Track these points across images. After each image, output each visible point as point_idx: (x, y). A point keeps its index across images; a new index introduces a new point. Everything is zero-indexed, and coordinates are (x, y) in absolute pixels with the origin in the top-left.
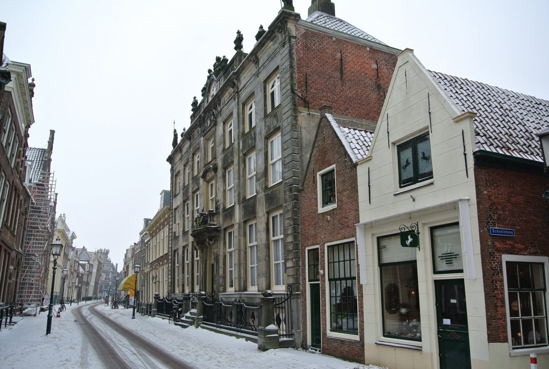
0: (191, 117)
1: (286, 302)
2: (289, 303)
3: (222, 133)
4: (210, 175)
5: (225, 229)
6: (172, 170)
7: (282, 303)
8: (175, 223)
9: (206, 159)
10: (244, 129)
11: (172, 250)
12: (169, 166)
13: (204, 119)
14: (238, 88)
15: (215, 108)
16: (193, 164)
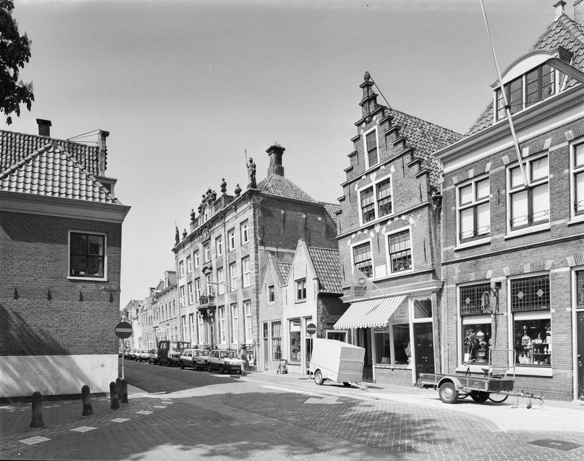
0: (191, 224)
4: (207, 271)
5: (219, 307)
6: (176, 258)
8: (181, 297)
10: (229, 248)
13: (202, 231)
16: (194, 259)
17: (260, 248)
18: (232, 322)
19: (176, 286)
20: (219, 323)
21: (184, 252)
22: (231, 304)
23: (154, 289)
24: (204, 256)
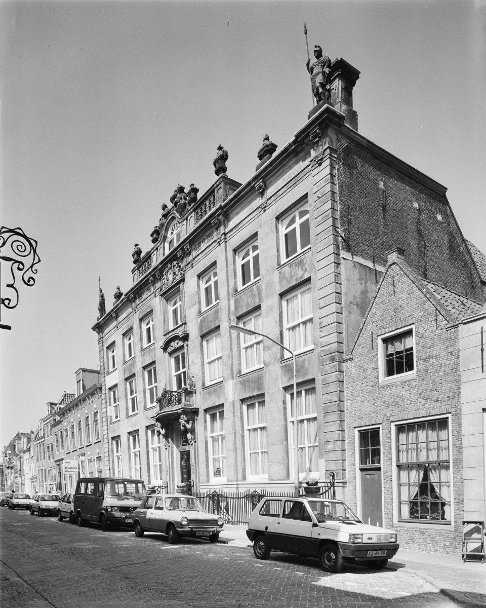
3: (196, 289)
4: (175, 345)
5: (206, 411)
6: (101, 340)
8: (110, 405)
9: (166, 325)
10: (236, 284)
12: (95, 334)
16: (141, 332)
17: (343, 254)
18: (243, 436)
19: (101, 389)
20: (206, 443)
21: (117, 327)
22: (242, 401)
23: (56, 404)
24: (165, 320)
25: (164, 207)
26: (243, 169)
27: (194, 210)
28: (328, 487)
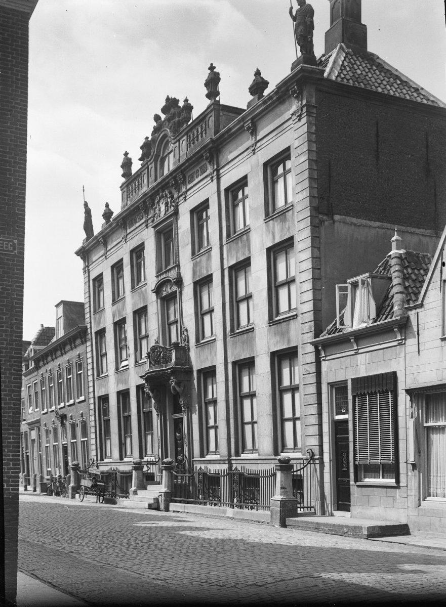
1: (305, 468)
2: (309, 469)
6: (87, 270)
7: (300, 470)
11: (94, 397)
12: (79, 262)
14: (218, 166)
15: (178, 188)
25: (157, 118)
26: (235, 94)
27: (187, 134)
28: (304, 463)
